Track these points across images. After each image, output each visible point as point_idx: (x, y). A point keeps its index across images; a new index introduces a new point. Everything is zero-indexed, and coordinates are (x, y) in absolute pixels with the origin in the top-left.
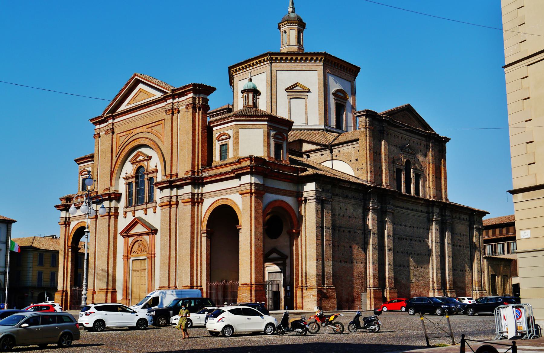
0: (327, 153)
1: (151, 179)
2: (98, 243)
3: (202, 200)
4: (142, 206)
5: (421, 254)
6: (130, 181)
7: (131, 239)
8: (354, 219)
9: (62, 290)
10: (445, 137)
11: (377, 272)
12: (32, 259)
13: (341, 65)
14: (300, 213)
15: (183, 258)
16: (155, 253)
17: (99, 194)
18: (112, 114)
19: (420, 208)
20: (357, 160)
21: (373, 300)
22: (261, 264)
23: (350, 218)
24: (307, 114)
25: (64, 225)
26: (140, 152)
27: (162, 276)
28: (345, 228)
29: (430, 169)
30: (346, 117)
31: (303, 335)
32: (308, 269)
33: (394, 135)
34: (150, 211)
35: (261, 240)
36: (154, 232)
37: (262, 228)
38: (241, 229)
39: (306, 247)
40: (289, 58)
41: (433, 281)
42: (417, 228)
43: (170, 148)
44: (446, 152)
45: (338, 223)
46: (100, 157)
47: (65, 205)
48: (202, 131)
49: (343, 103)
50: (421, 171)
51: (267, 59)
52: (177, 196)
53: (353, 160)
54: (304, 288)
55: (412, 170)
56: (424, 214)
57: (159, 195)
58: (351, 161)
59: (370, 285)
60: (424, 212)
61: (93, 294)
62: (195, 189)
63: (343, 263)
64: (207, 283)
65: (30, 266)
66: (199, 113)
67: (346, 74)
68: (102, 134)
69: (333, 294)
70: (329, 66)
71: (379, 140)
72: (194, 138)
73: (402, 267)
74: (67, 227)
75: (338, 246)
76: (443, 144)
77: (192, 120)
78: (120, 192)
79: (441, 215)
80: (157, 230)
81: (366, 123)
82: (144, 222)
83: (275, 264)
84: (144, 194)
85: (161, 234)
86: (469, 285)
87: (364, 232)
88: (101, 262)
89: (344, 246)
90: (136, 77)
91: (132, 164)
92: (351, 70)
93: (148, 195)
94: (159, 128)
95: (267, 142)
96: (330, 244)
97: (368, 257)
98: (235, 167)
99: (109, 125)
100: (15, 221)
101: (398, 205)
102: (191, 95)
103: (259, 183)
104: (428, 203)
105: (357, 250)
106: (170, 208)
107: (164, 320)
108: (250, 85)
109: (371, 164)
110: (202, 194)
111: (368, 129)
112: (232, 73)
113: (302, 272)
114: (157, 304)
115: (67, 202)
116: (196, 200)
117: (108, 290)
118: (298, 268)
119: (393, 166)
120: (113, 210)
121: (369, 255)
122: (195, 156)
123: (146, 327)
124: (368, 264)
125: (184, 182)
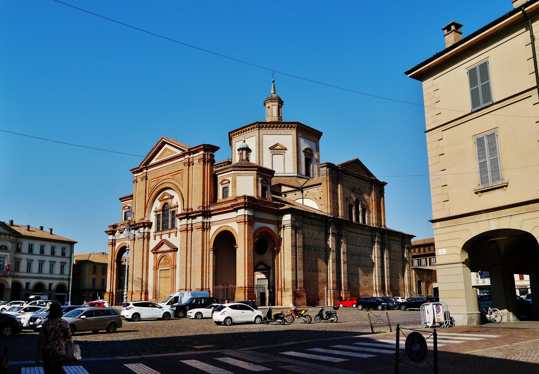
0: (299, 193)
1: (173, 212)
2: (135, 257)
3: (210, 227)
4: (167, 231)
5: (367, 266)
6: (158, 213)
7: (159, 255)
9: (109, 291)
10: (384, 182)
11: (335, 279)
12: (88, 269)
13: (309, 131)
14: (280, 236)
15: (196, 269)
16: (176, 265)
17: (136, 223)
18: (146, 166)
19: (366, 233)
20: (320, 198)
21: (332, 299)
22: (252, 273)
24: (284, 165)
25: (111, 245)
26: (166, 193)
27: (181, 281)
29: (373, 204)
30: (313, 167)
31: (282, 325)
32: (286, 276)
33: (347, 181)
34: (173, 235)
35: (252, 255)
36: (175, 250)
37: (252, 247)
38: (237, 248)
39: (284, 261)
40: (272, 125)
41: (376, 286)
42: (364, 247)
43: (187, 190)
44: (384, 193)
45: (307, 243)
46: (137, 196)
47: (112, 230)
48: (210, 177)
49: (311, 158)
50: (366, 206)
51: (256, 126)
52: (192, 224)
53: (318, 198)
54: (283, 290)
55: (360, 205)
56: (369, 237)
57: (179, 223)
58: (316, 199)
59: (330, 288)
60: (369, 236)
61: (132, 295)
62: (205, 219)
63: (311, 272)
64: (213, 287)
65: (87, 275)
66: (207, 165)
67: (313, 137)
68: (139, 180)
70: (300, 132)
71: (336, 184)
72: (204, 182)
74: (114, 247)
75: (307, 260)
76: (382, 187)
77: (202, 170)
78: (151, 221)
79: (381, 238)
80: (178, 248)
81: (327, 172)
82: (168, 243)
83: (262, 273)
84: (168, 223)
85: (180, 251)
86: (402, 288)
87: (326, 250)
88: (137, 271)
89: (312, 260)
90: (163, 140)
91: (160, 201)
92: (316, 134)
93: (171, 223)
94: (179, 176)
95: (256, 186)
96: (301, 259)
97: (328, 268)
98: (233, 203)
99: (144, 174)
100: (76, 243)
102: (202, 152)
103: (251, 215)
104: (372, 229)
105: (320, 263)
106: (187, 233)
107: (182, 313)
108: (244, 145)
109: (330, 201)
110: (210, 223)
111: (328, 176)
112: (231, 137)
113: (281, 279)
114: (177, 302)
115: (113, 229)
116: (205, 227)
117: (142, 291)
118: (279, 276)
119: (347, 202)
120: (146, 234)
121: (329, 267)
122: (205, 196)
123: (170, 318)
124: (329, 273)
125: (197, 214)
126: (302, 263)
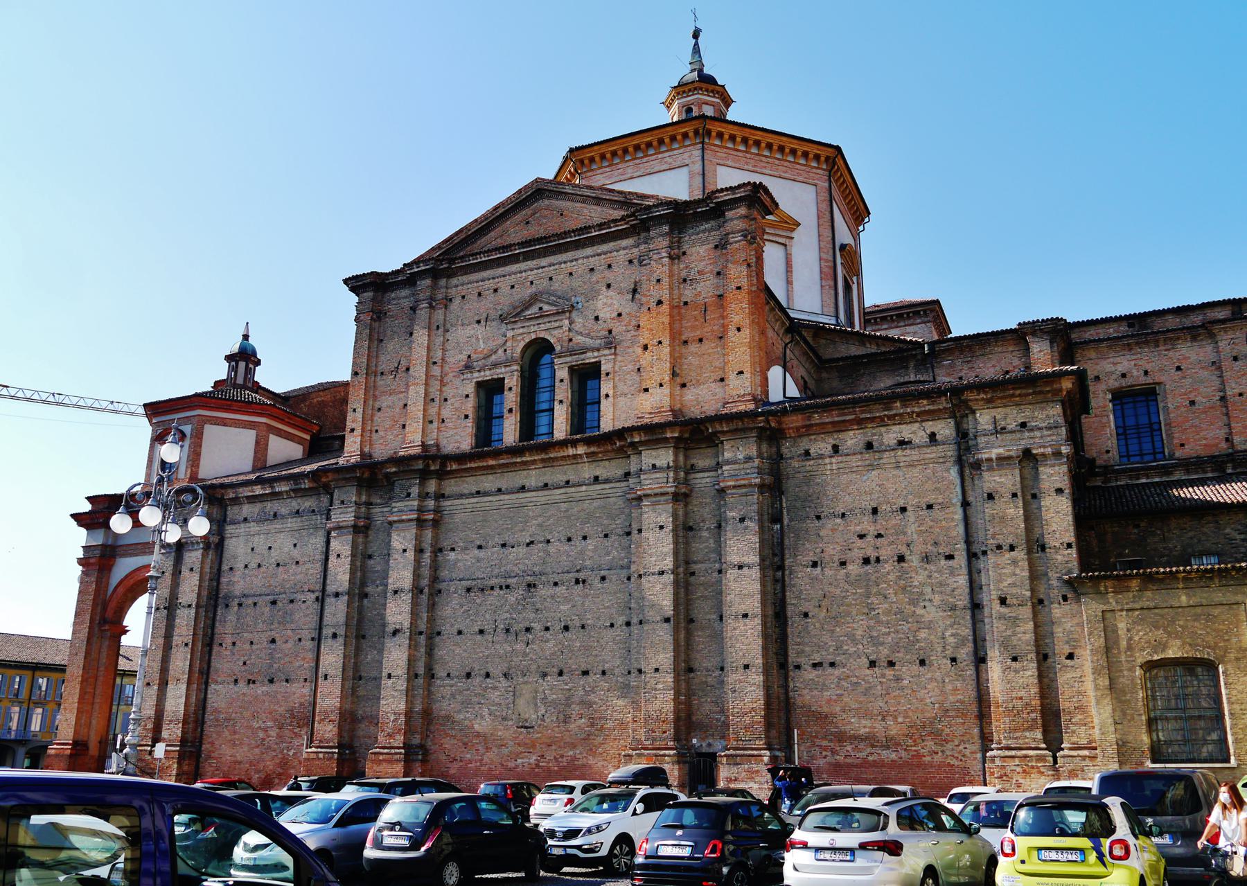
8: (294, 566)
23: (281, 568)
28: (260, 595)
63: (242, 684)
69: (167, 765)
73: (476, 681)
75: (234, 644)
89: (252, 643)
101: (474, 489)
126: (185, 659)
